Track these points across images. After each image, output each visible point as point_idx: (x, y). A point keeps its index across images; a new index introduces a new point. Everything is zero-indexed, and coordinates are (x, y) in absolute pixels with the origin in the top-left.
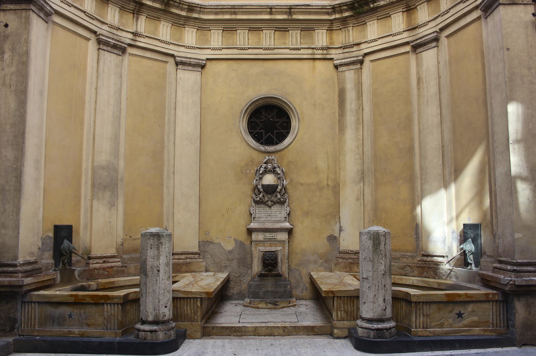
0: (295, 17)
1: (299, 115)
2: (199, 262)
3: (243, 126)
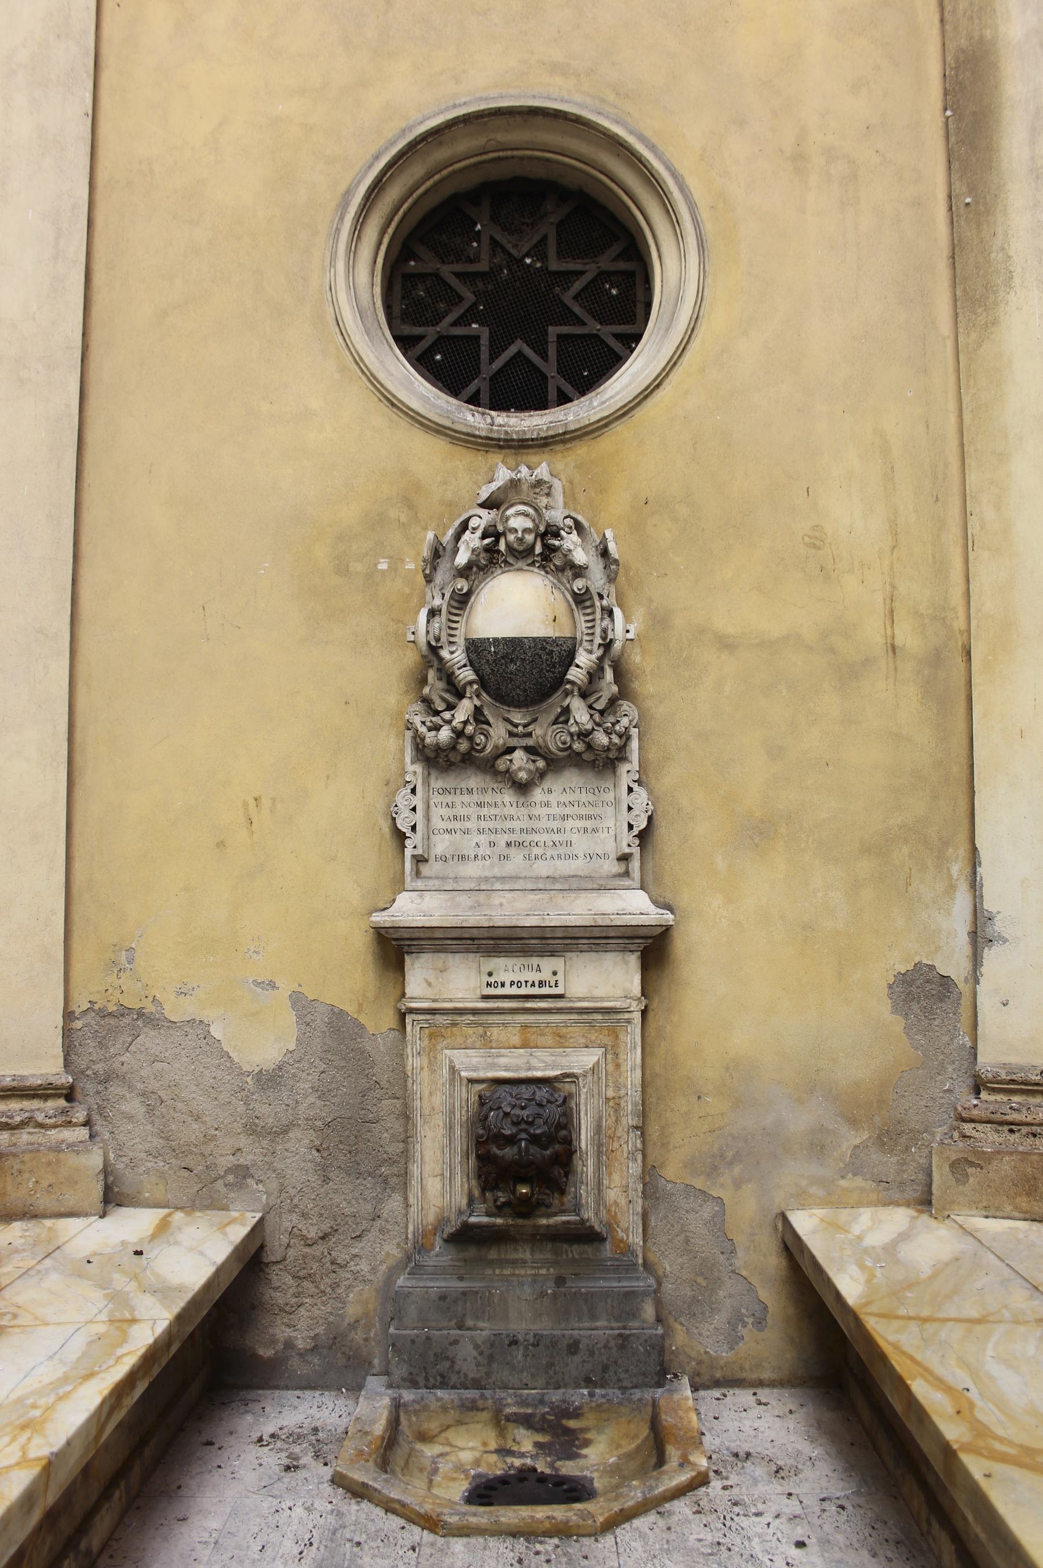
1: (704, 214)
2: (57, 1149)
3: (352, 286)
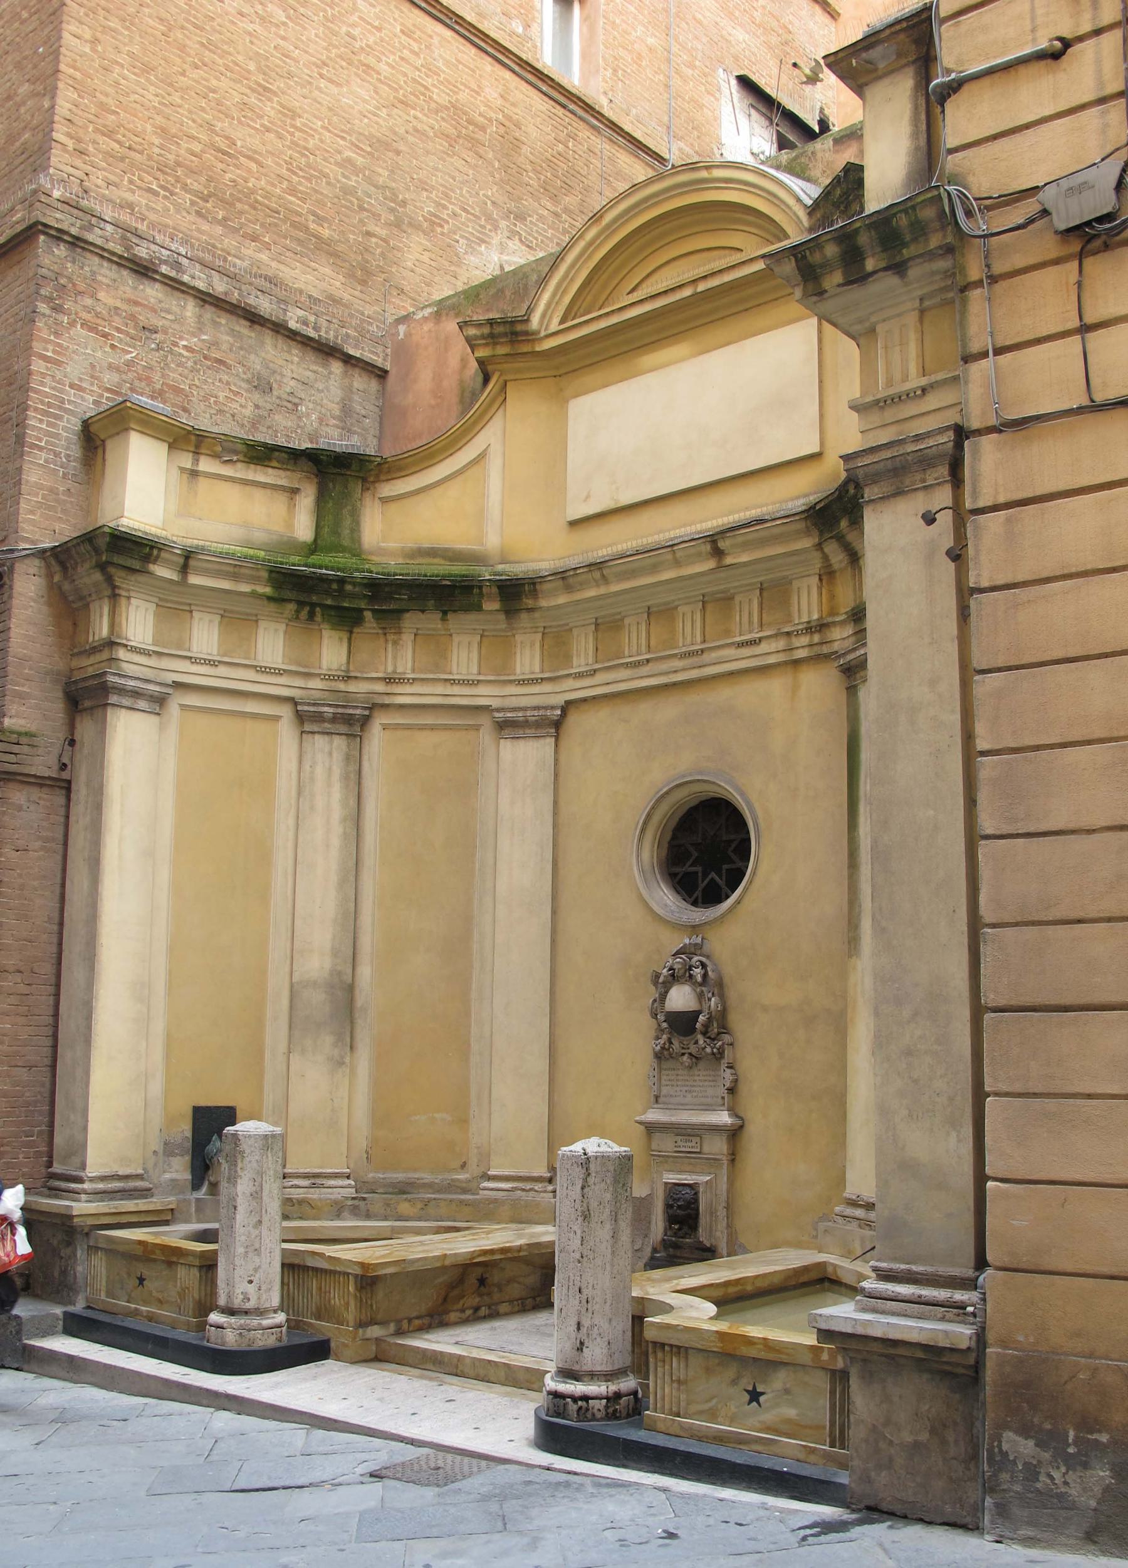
0: (729, 560)
